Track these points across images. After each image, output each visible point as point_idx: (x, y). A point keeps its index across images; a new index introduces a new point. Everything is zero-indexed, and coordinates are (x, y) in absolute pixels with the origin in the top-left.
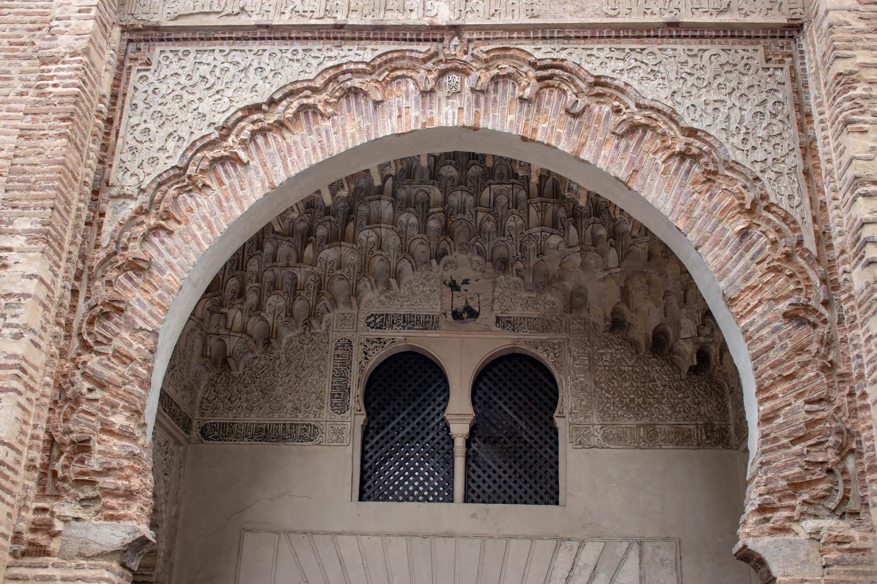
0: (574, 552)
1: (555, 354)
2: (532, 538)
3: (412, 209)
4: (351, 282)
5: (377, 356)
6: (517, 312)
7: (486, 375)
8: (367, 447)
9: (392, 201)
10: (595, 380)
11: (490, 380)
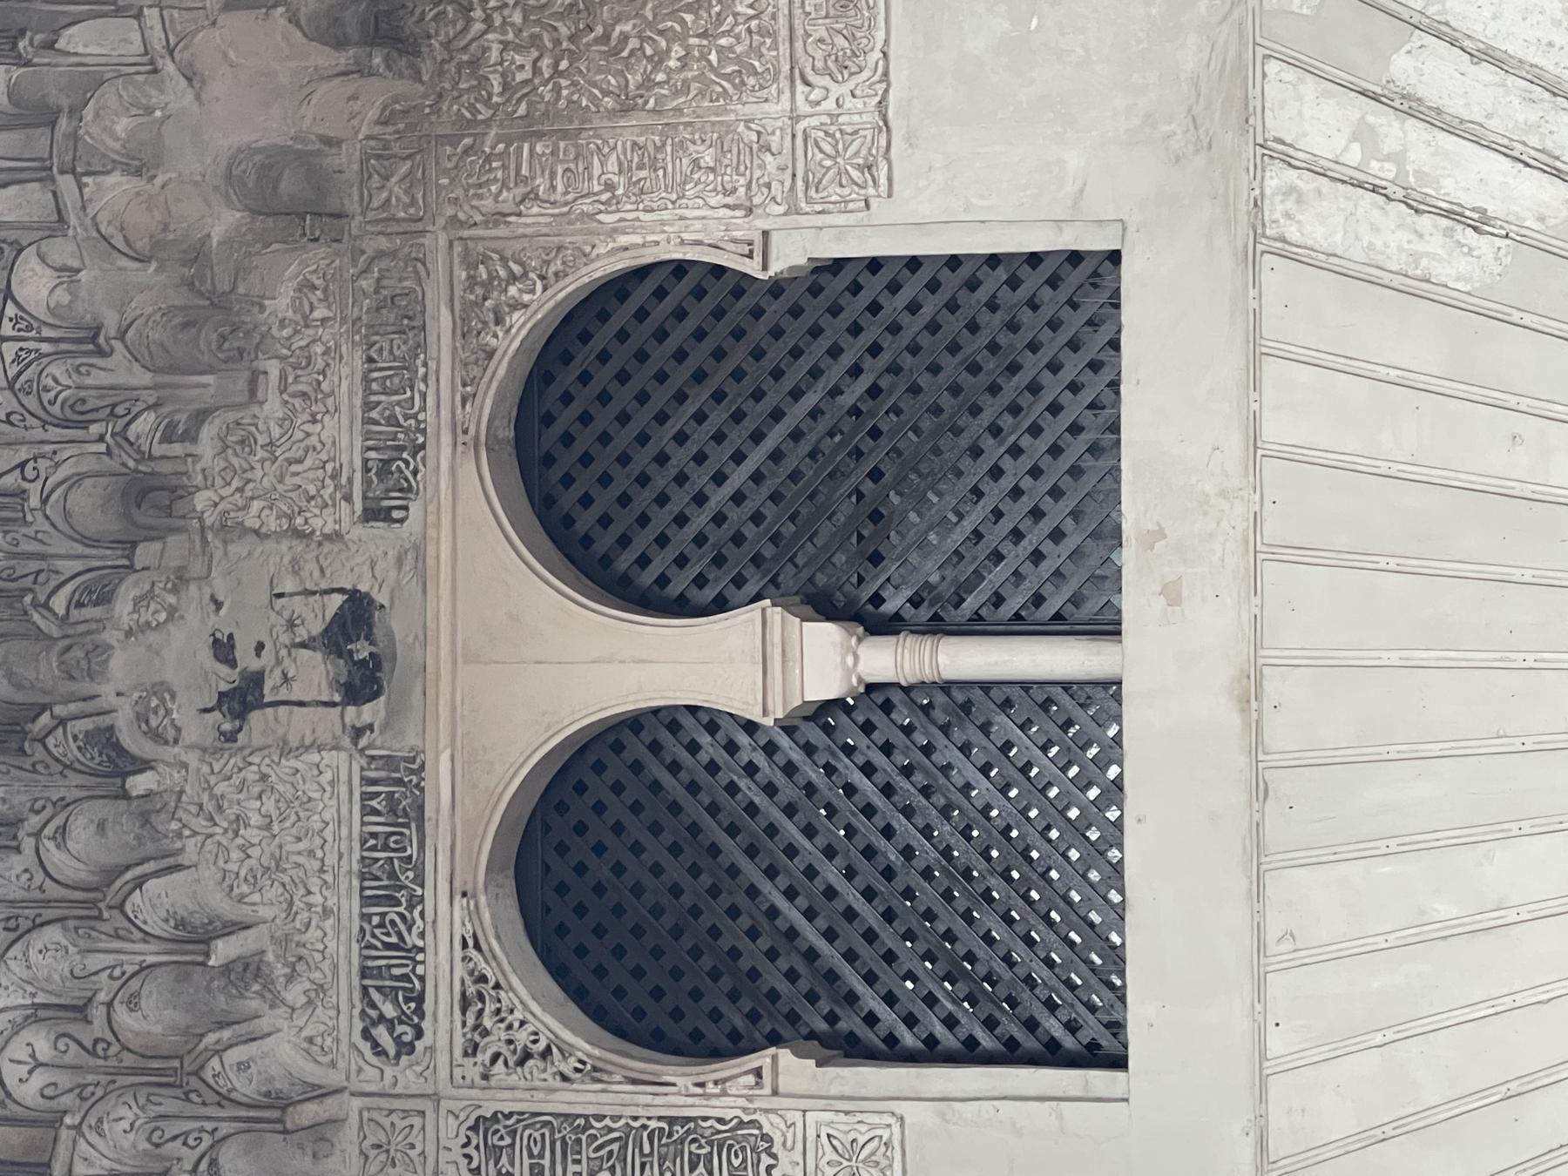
0: (1307, 182)
1: (513, 279)
2: (1256, 353)
4: (225, 1128)
5: (536, 1007)
6: (343, 437)
7: (606, 561)
8: (908, 1039)
10: (612, 113)
11: (624, 541)
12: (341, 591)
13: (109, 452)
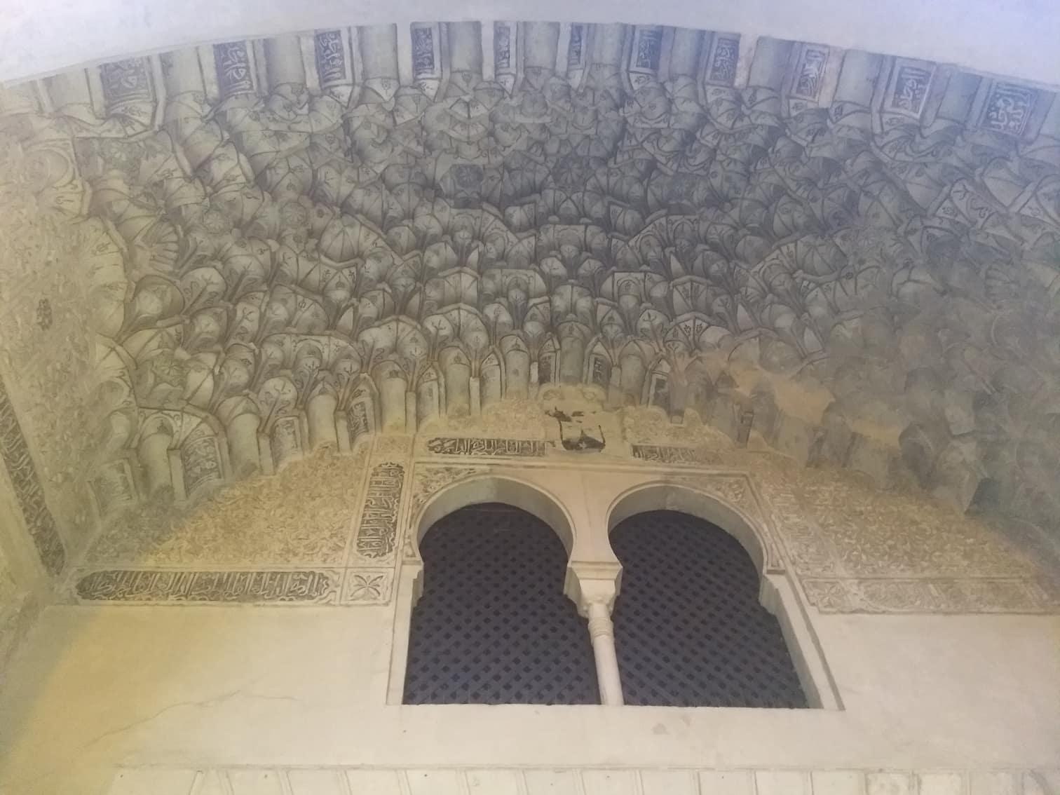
6: (662, 440)
9: (477, 279)
13: (656, 354)
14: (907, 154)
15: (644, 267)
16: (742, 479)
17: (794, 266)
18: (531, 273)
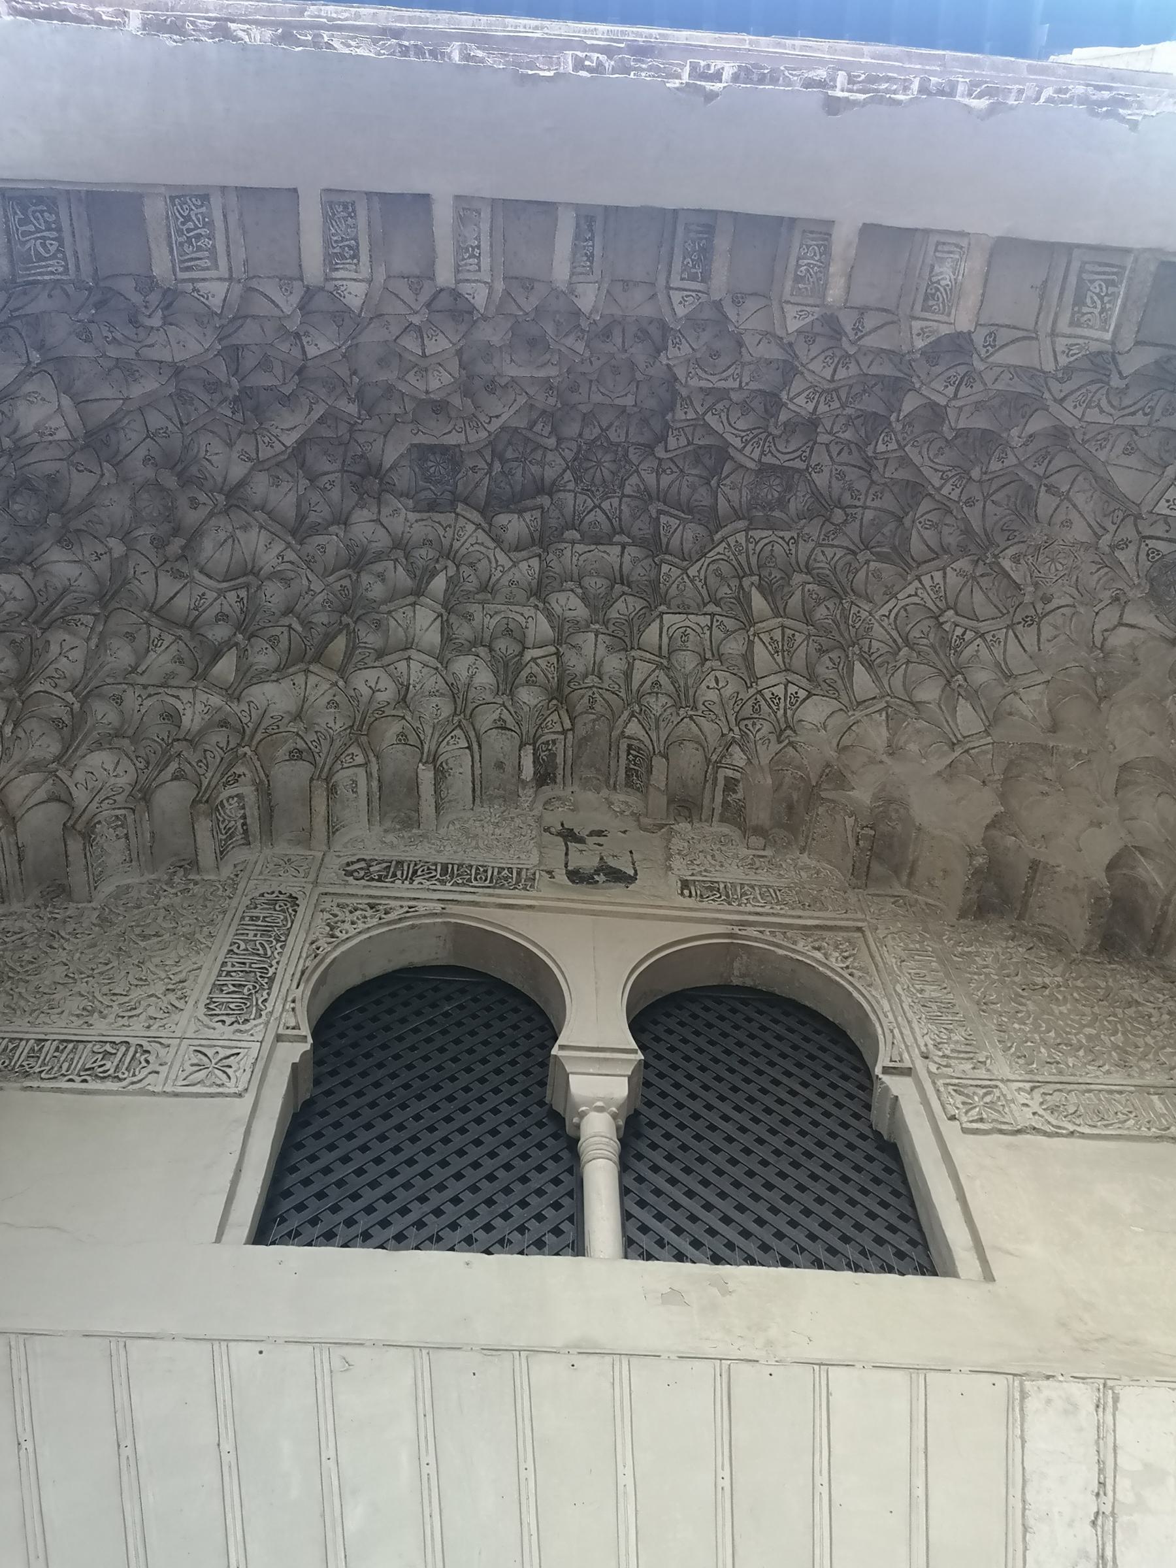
3: (482, 651)
6: (732, 874)
12: (636, 874)
13: (723, 735)
14: (1102, 411)
15: (711, 608)
16: (857, 935)
17: (942, 605)
18: (528, 611)
